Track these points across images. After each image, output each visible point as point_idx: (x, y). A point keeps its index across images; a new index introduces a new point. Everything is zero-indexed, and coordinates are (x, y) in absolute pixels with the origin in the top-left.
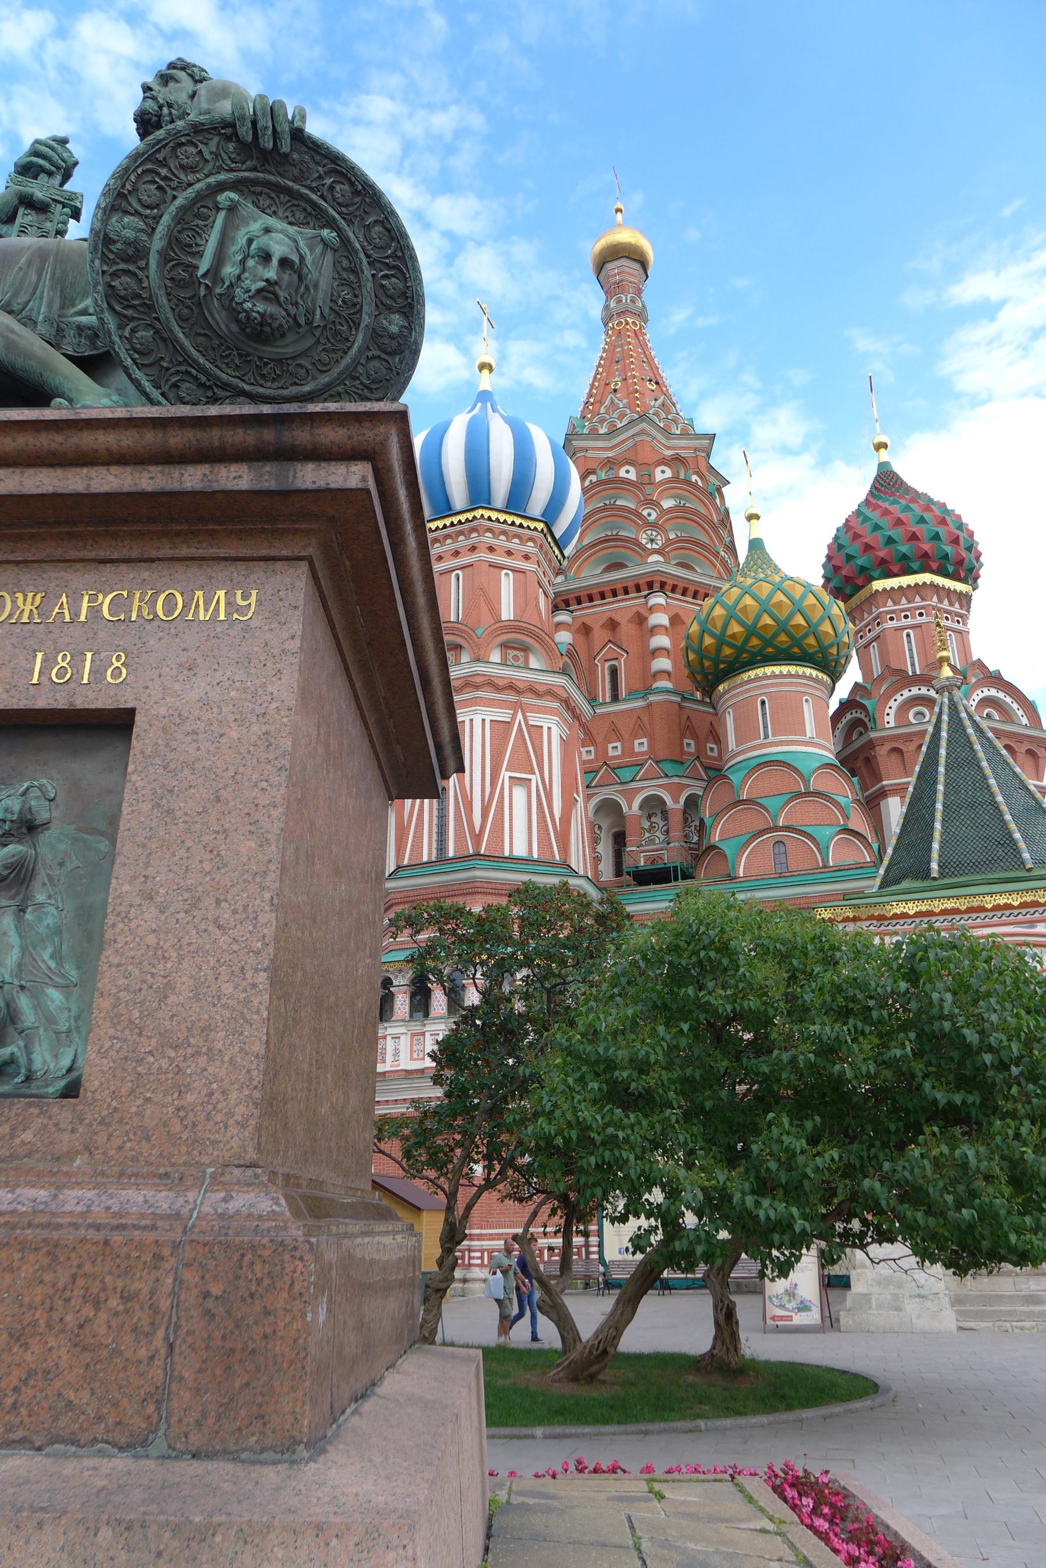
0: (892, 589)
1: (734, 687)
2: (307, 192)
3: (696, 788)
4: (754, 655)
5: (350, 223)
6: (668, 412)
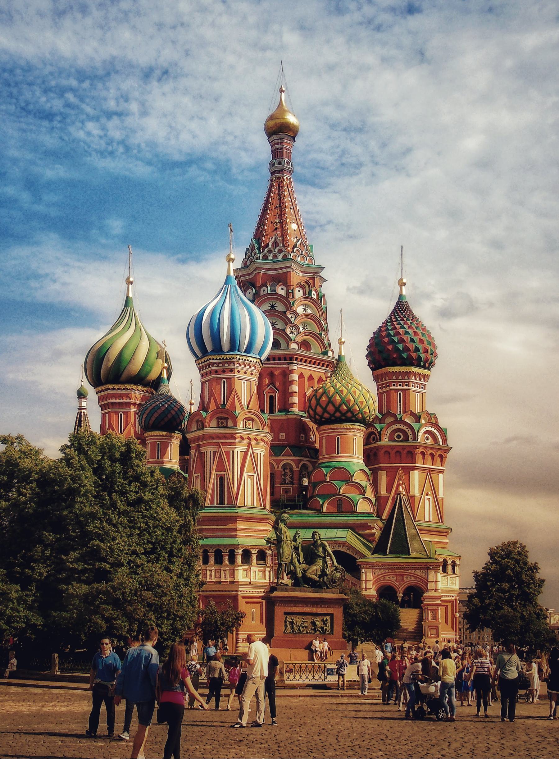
3: (305, 461)
4: (337, 418)
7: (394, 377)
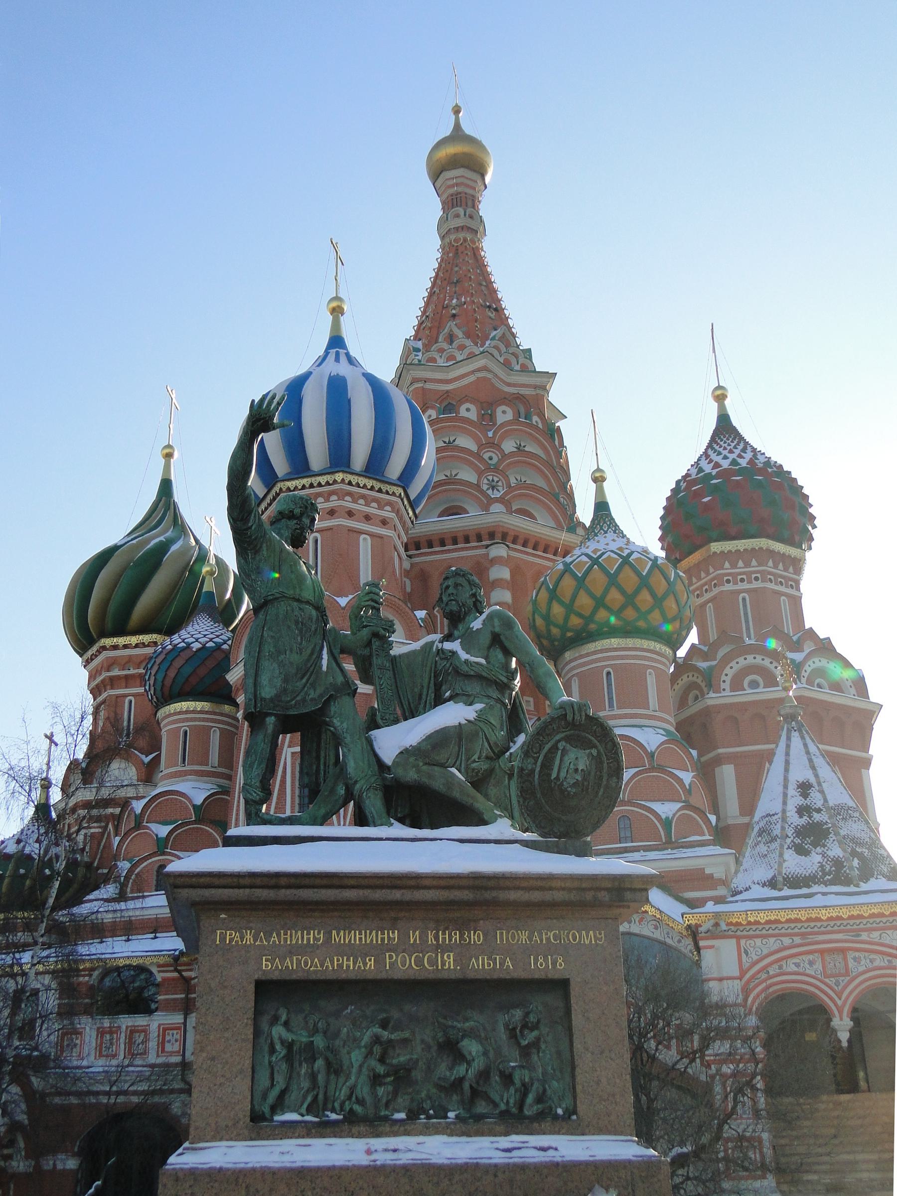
0: (730, 551)
1: (581, 657)
6: (508, 345)
7: (727, 565)
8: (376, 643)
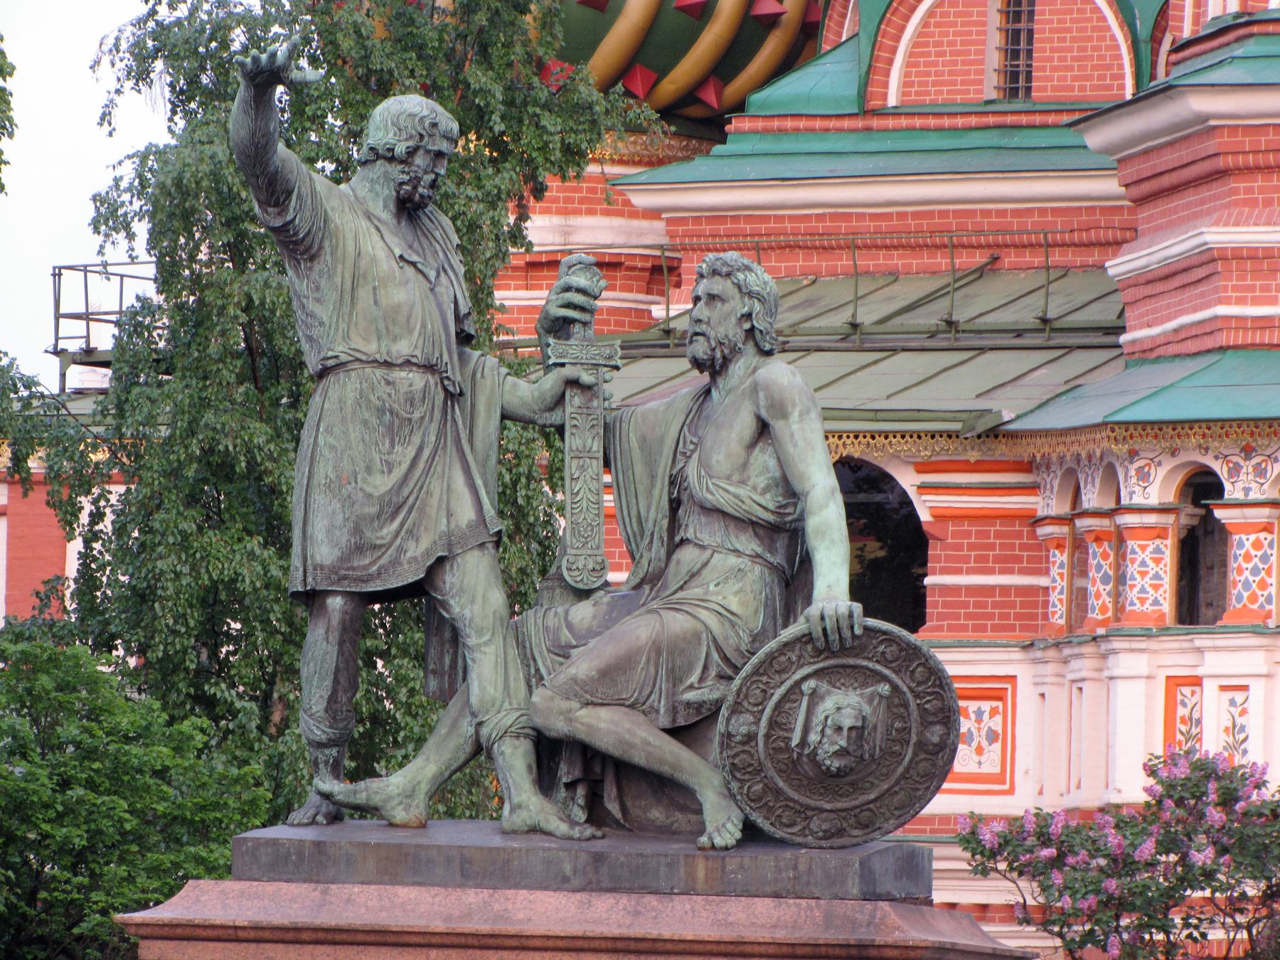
2: (865, 663)
5: (897, 672)
8: (574, 400)
